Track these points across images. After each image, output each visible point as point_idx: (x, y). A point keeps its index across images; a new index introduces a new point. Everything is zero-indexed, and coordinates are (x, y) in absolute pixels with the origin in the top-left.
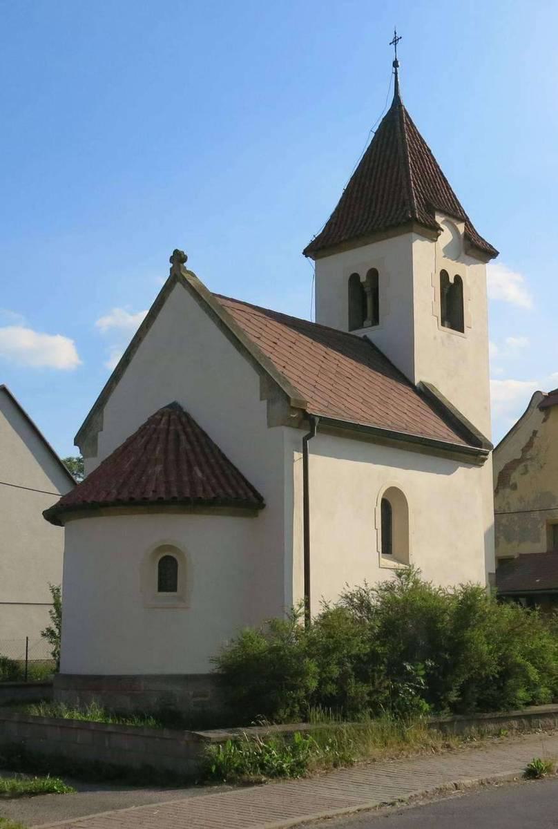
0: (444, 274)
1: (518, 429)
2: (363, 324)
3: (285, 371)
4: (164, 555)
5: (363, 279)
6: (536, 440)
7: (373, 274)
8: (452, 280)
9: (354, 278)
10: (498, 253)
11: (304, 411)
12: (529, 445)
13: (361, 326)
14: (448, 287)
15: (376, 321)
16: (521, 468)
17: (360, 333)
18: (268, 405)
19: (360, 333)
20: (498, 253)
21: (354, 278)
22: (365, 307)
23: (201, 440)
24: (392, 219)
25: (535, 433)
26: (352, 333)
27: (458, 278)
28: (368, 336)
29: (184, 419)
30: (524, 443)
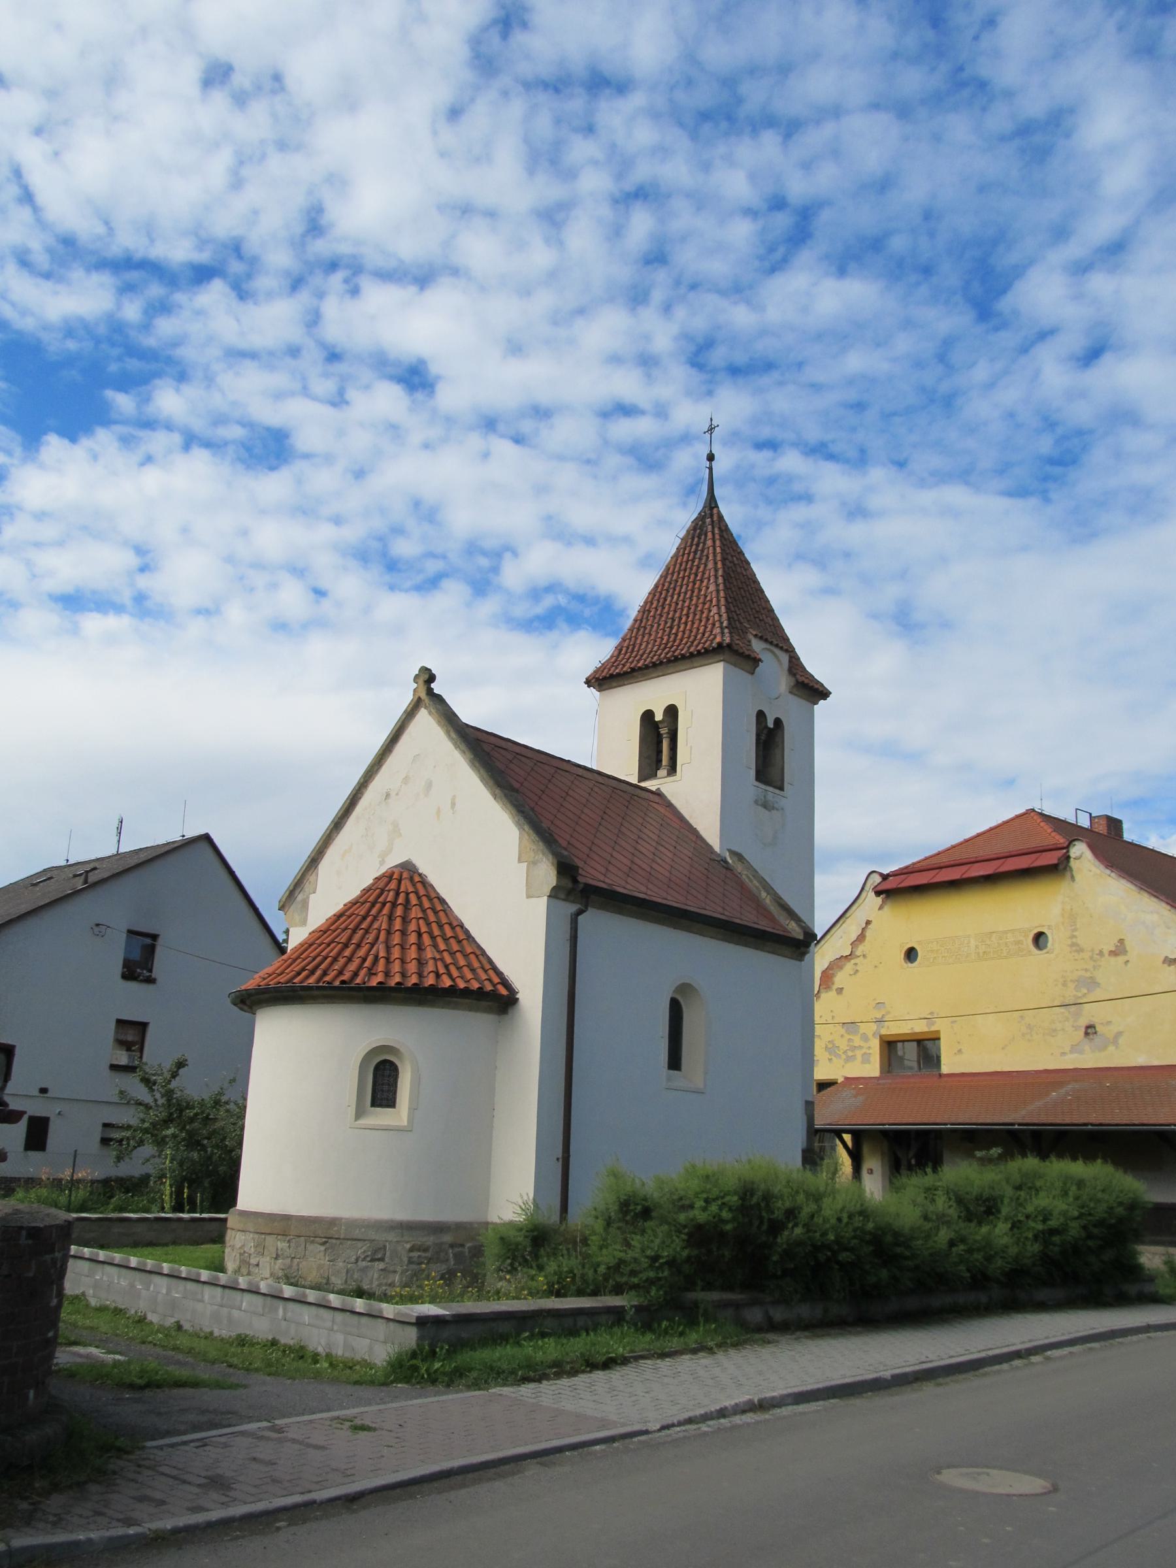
0: (761, 715)
1: (847, 918)
2: (656, 775)
3: (553, 828)
4: (381, 1059)
5: (659, 717)
6: (868, 933)
7: (672, 712)
8: (771, 725)
9: (648, 716)
10: (830, 693)
11: (304, 236)
12: (861, 938)
13: (653, 775)
14: (765, 732)
15: (673, 769)
16: (849, 967)
17: (651, 785)
18: (528, 867)
19: (651, 785)
20: (830, 693)
21: (648, 716)
22: (660, 752)
23: (436, 905)
24: (699, 643)
25: (868, 923)
26: (643, 784)
27: (778, 722)
28: (661, 789)
29: (417, 879)
30: (854, 937)
